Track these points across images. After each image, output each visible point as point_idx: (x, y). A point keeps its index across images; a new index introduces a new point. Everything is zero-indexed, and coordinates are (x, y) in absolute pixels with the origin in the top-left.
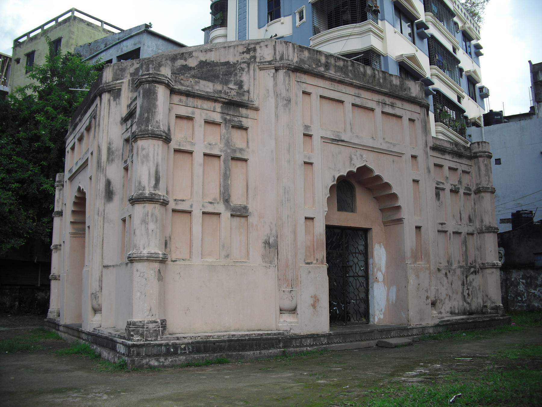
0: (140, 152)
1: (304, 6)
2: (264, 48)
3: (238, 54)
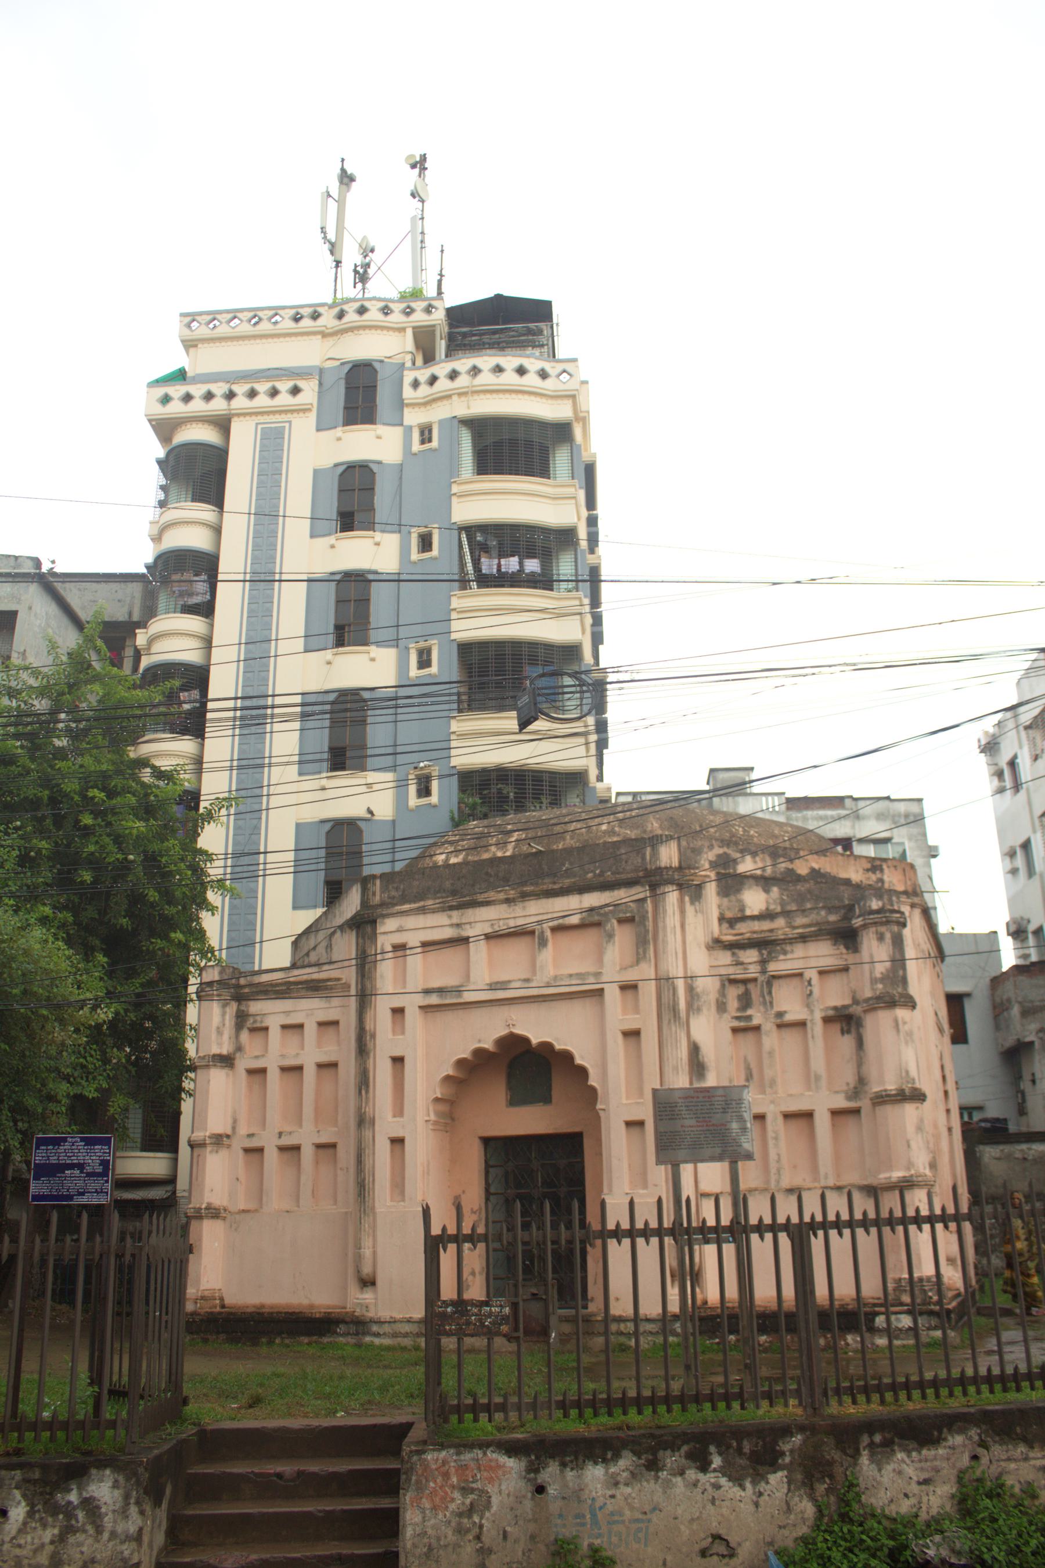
0: (901, 1026)
1: (435, 641)
2: (892, 869)
3: (861, 871)
